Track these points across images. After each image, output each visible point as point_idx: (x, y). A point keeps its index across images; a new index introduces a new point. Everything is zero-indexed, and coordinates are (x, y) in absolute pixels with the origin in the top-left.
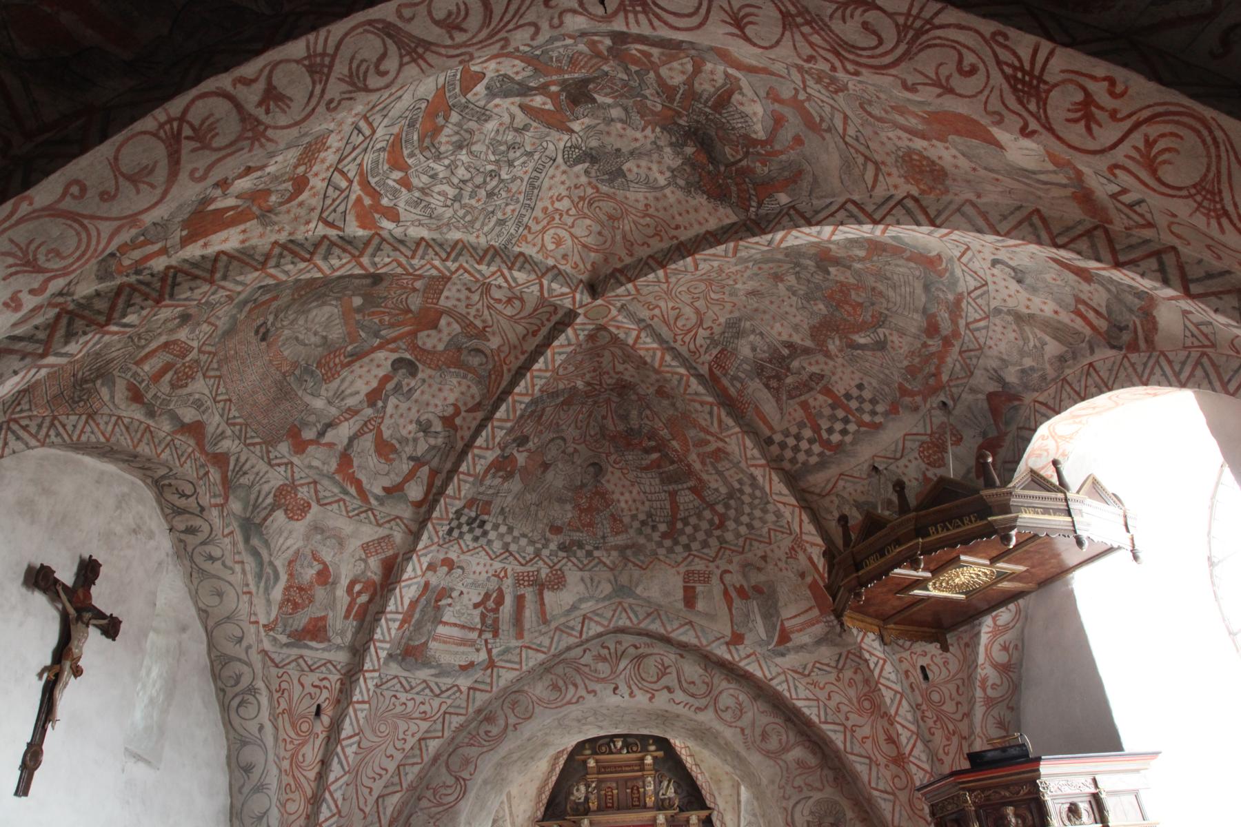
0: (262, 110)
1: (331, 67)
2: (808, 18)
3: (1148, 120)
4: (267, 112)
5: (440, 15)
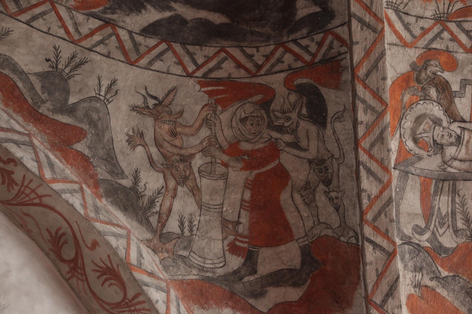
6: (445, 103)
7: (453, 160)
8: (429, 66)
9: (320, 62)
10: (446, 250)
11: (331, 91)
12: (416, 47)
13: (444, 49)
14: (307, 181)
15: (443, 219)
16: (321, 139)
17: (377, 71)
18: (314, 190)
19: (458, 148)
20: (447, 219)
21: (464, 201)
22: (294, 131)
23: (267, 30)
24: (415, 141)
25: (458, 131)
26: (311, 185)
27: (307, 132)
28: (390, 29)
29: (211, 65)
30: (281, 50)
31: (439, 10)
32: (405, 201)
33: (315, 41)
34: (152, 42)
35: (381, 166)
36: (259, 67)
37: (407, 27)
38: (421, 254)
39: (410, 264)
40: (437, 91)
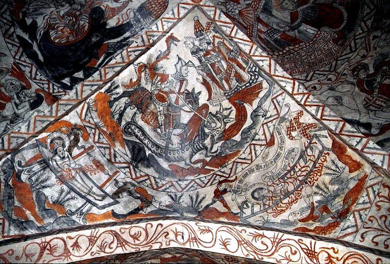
0: (72, 248)
1: (96, 241)
2: (245, 242)
3: (347, 258)
4: (73, 250)
5: (132, 233)
9: (53, 96)
11: (46, 104)
16: (27, 111)
18: (5, 120)
22: (22, 102)
23: (50, 75)
24: (51, 142)
25: (66, 156)
29: (23, 63)
30: (47, 82)
34: (16, 40)
36: (35, 79)
37: (86, 115)
39: (4, 168)
40: (74, 138)
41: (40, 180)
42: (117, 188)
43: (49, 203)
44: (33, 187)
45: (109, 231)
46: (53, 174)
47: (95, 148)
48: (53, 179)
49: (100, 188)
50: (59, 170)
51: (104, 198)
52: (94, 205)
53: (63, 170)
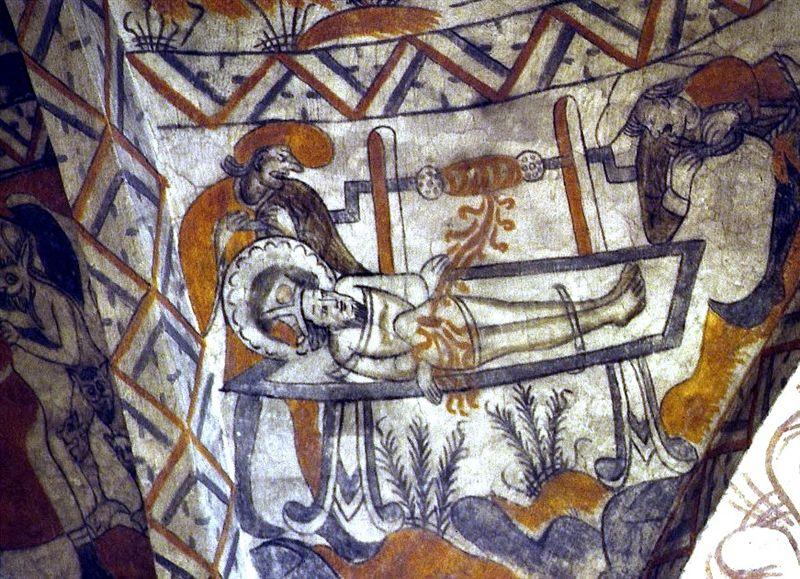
6: (315, 239)
7: (357, 357)
8: (265, 162)
10: (360, 549)
12: (229, 125)
13: (297, 118)
14: (71, 412)
15: (350, 483)
17: (115, 215)
18: (87, 431)
19: (363, 331)
20: (358, 485)
21: (392, 444)
22: (28, 306)
24: (264, 326)
25: (358, 296)
26: (80, 420)
27: (52, 307)
28: (158, 96)
31: (272, 30)
32: (260, 456)
33: (25, 115)
35: (161, 410)
37: (199, 82)
38: (308, 561)
40: (293, 215)
41: (409, 471)
42: (631, 188)
43: (524, 509)
44: (425, 519)
45: (777, 435)
46: (412, 402)
47: (385, 133)
48: (438, 419)
49: (587, 259)
50: (405, 365)
51: (636, 285)
52: (640, 349)
53: (414, 351)
